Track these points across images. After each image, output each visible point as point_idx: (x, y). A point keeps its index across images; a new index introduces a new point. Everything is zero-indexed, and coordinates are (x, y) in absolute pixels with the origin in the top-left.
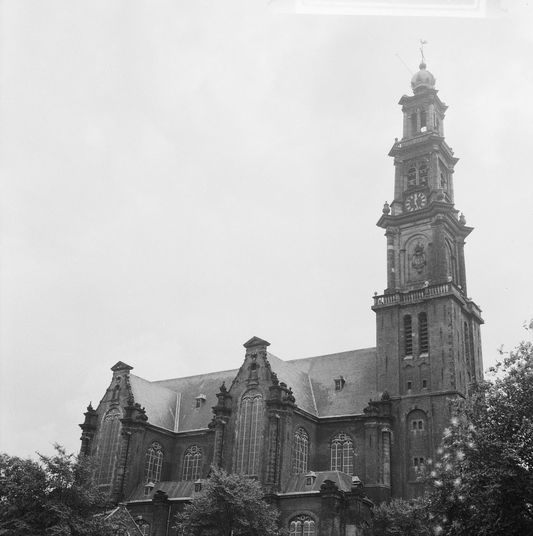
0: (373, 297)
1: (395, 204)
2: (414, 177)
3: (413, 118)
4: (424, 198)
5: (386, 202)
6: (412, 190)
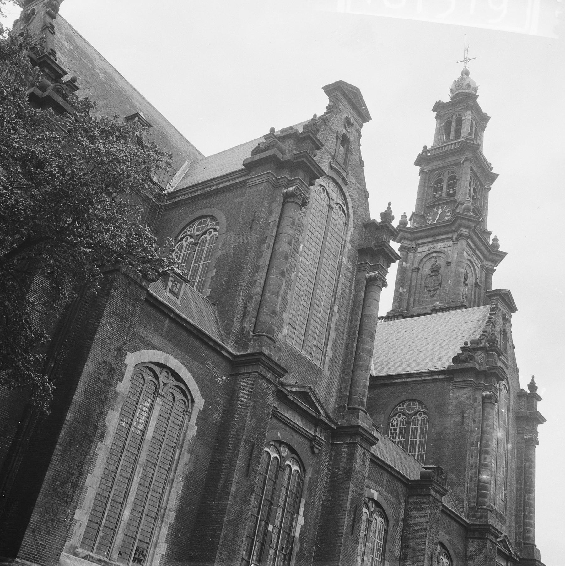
2: (441, 188)
3: (448, 125)
4: (449, 211)
5: (405, 213)
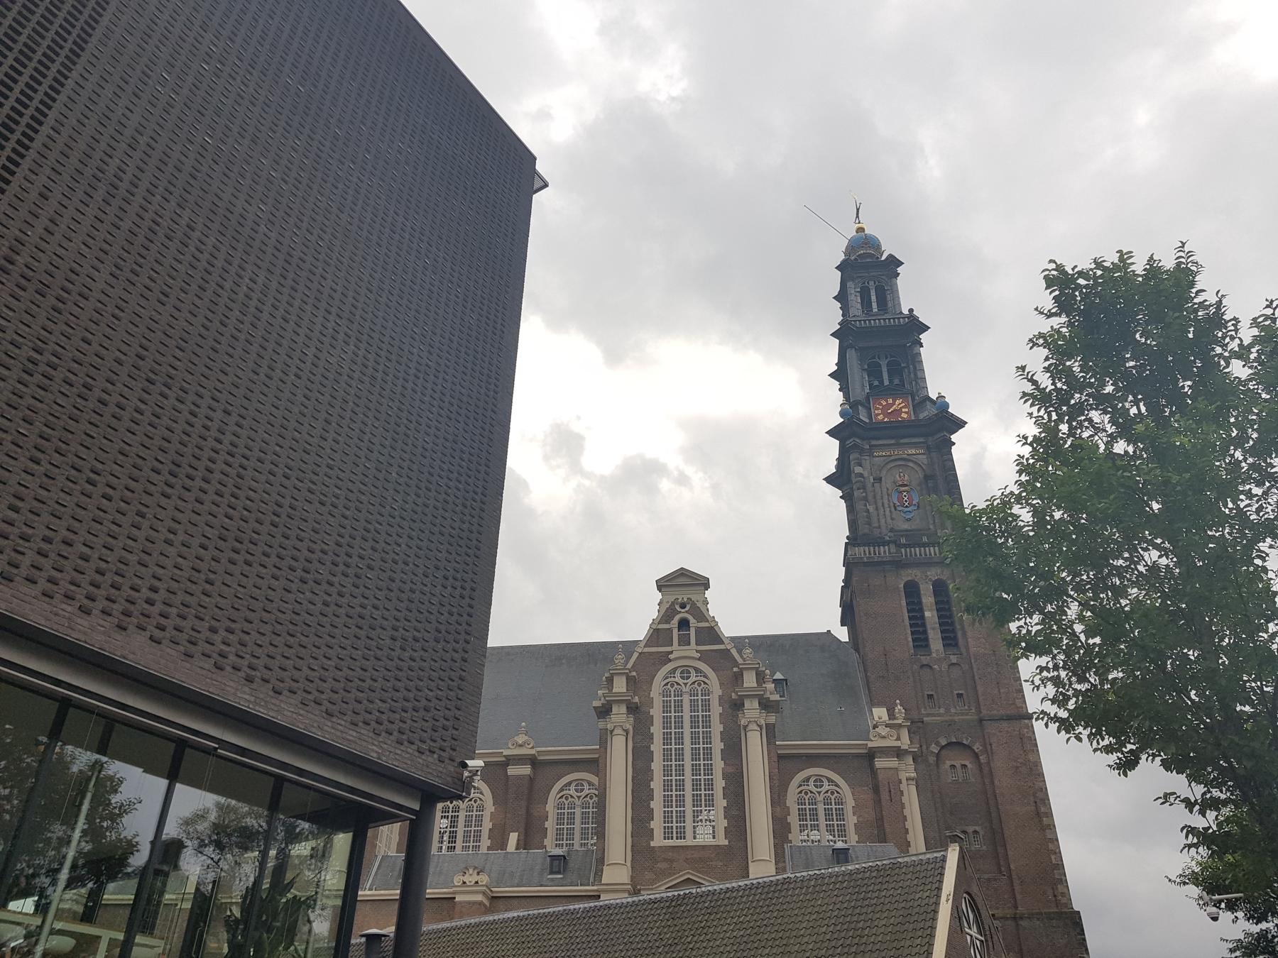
6: (878, 391)
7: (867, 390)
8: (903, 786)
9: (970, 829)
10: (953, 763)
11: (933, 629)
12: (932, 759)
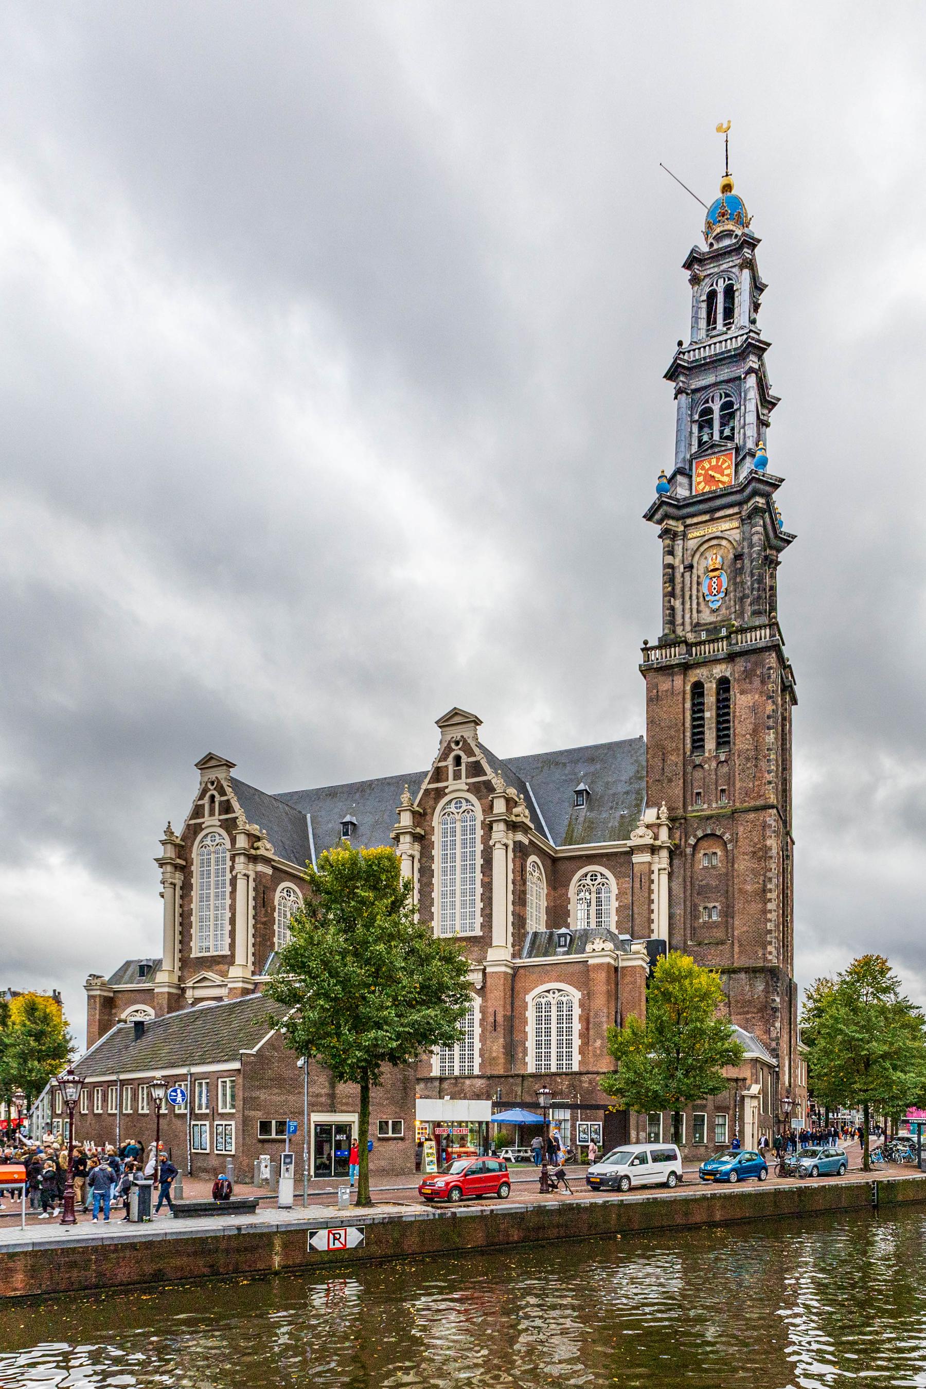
0: (643, 650)
1: (679, 478)
3: (712, 295)
5: (663, 472)
6: (705, 448)
7: (694, 449)
8: (655, 877)
9: (711, 905)
10: (706, 852)
11: (710, 729)
12: (689, 850)
